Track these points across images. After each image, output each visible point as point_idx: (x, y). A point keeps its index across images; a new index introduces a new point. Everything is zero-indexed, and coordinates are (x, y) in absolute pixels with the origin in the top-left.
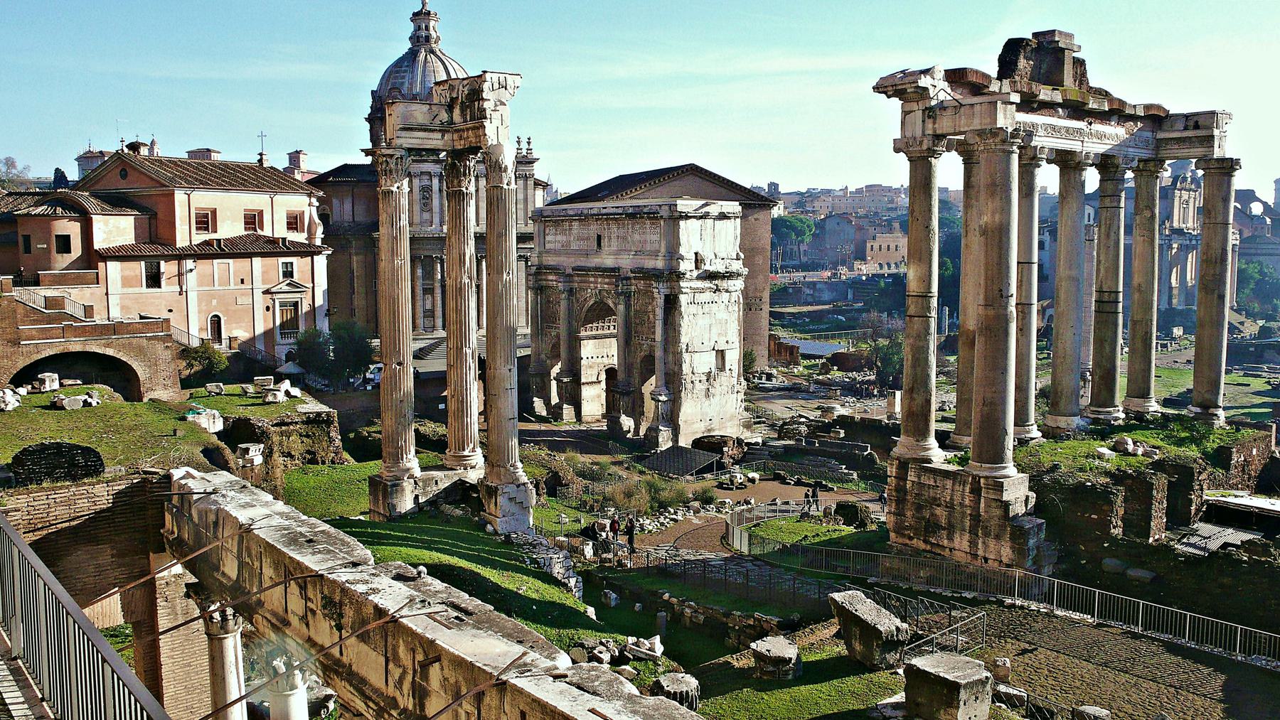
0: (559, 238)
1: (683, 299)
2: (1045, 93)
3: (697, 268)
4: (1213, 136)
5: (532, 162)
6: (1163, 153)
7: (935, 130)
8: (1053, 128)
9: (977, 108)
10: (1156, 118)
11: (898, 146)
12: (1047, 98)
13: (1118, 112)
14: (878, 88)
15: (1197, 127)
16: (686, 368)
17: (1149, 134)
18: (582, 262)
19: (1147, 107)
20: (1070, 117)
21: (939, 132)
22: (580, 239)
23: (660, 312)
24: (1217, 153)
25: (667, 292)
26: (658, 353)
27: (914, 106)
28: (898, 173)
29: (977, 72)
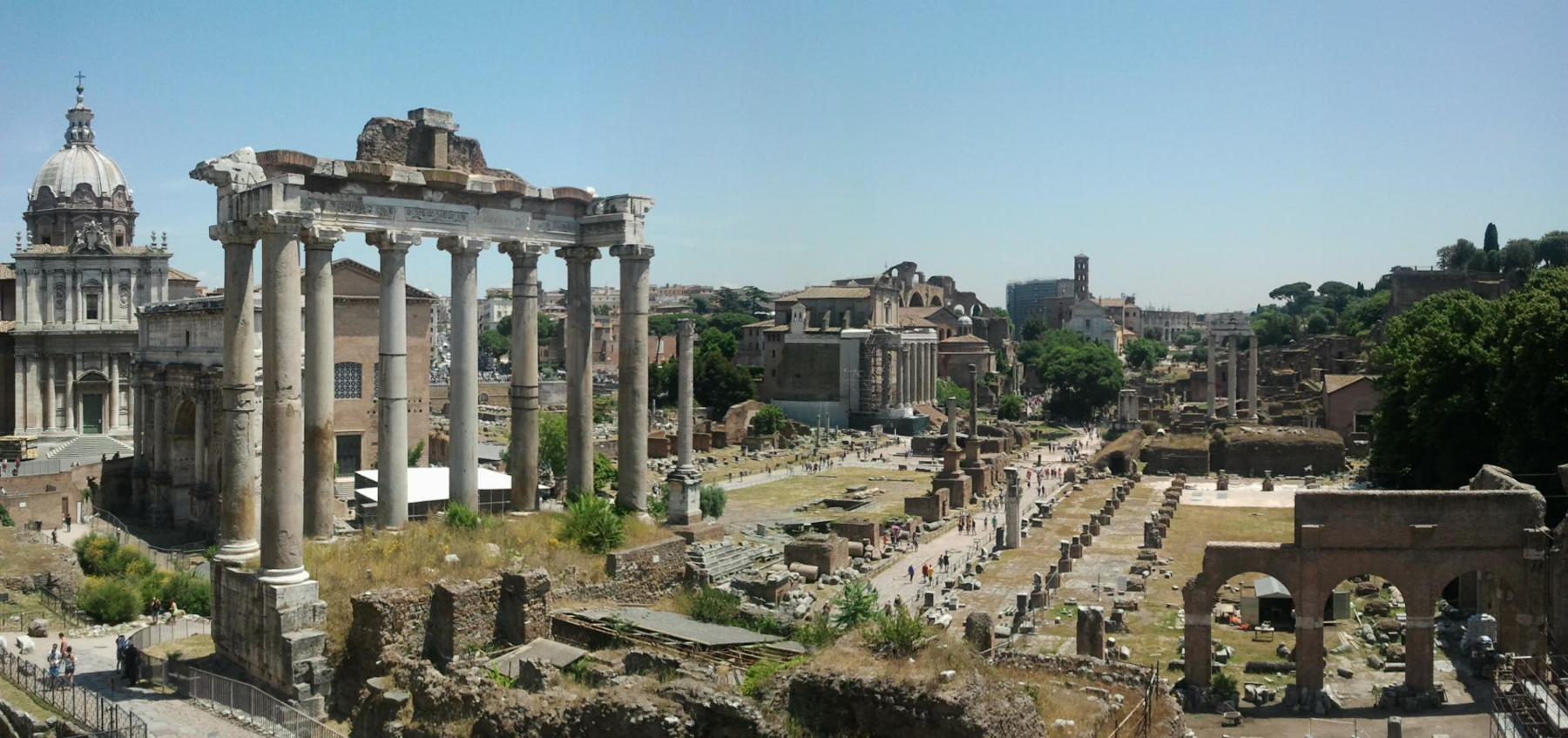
0: (160, 335)
2: (400, 173)
4: (623, 222)
5: (166, 258)
6: (588, 241)
8: (421, 211)
10: (572, 204)
13: (509, 195)
14: (194, 175)
17: (571, 219)
18: (173, 358)
19: (557, 191)
20: (446, 200)
22: (174, 336)
24: (630, 239)
29: (295, 153)
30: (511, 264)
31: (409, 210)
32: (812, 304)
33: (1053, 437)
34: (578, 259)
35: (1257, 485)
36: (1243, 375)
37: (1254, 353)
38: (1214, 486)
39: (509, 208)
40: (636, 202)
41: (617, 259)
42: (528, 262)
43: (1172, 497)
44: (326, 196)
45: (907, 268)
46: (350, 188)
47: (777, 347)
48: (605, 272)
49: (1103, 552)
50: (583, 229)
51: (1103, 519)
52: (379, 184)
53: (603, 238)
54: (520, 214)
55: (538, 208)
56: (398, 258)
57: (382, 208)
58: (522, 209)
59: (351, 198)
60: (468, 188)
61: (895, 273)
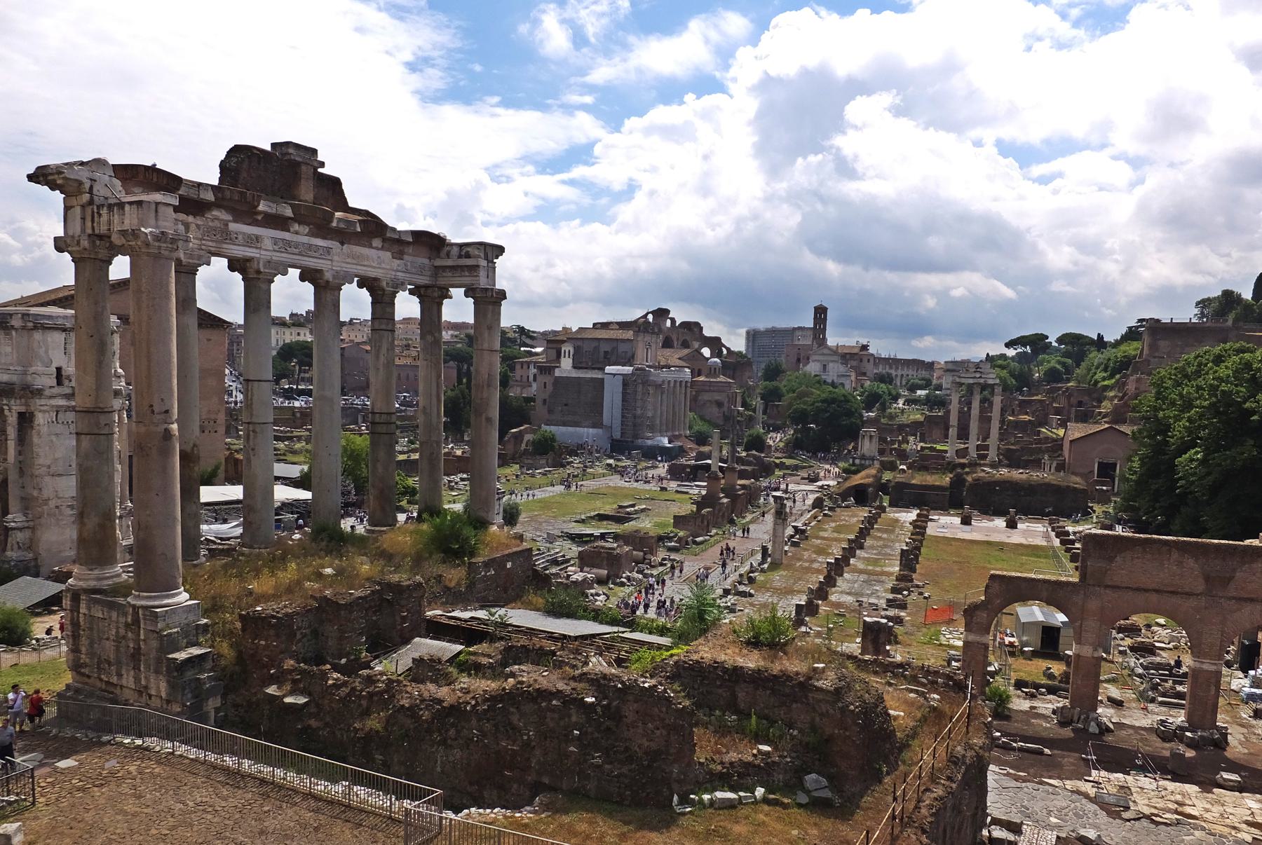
1: (40, 419)
3: (59, 383)
6: (441, 282)
7: (93, 228)
8: (288, 243)
9: (127, 207)
11: (62, 245)
12: (274, 211)
15: (468, 256)
16: (47, 493)
17: (426, 261)
21: (97, 232)
23: (12, 432)
24: (483, 282)
25: (23, 409)
26: (13, 476)
27: (73, 201)
28: (64, 272)
30: (370, 299)
31: (275, 241)
32: (579, 343)
33: (796, 468)
34: (431, 298)
35: (1000, 523)
36: (985, 420)
37: (997, 400)
38: (957, 520)
39: (371, 246)
40: (489, 250)
41: (471, 300)
42: (387, 299)
43: (919, 527)
44: (190, 219)
45: (662, 313)
46: (216, 213)
47: (548, 379)
48: (458, 309)
49: (861, 572)
50: (437, 270)
51: (856, 544)
52: (247, 213)
53: (457, 280)
54: (381, 253)
55: (396, 248)
56: (264, 286)
57: (249, 236)
58: (382, 248)
59: (216, 223)
60: (334, 224)
61: (650, 317)
